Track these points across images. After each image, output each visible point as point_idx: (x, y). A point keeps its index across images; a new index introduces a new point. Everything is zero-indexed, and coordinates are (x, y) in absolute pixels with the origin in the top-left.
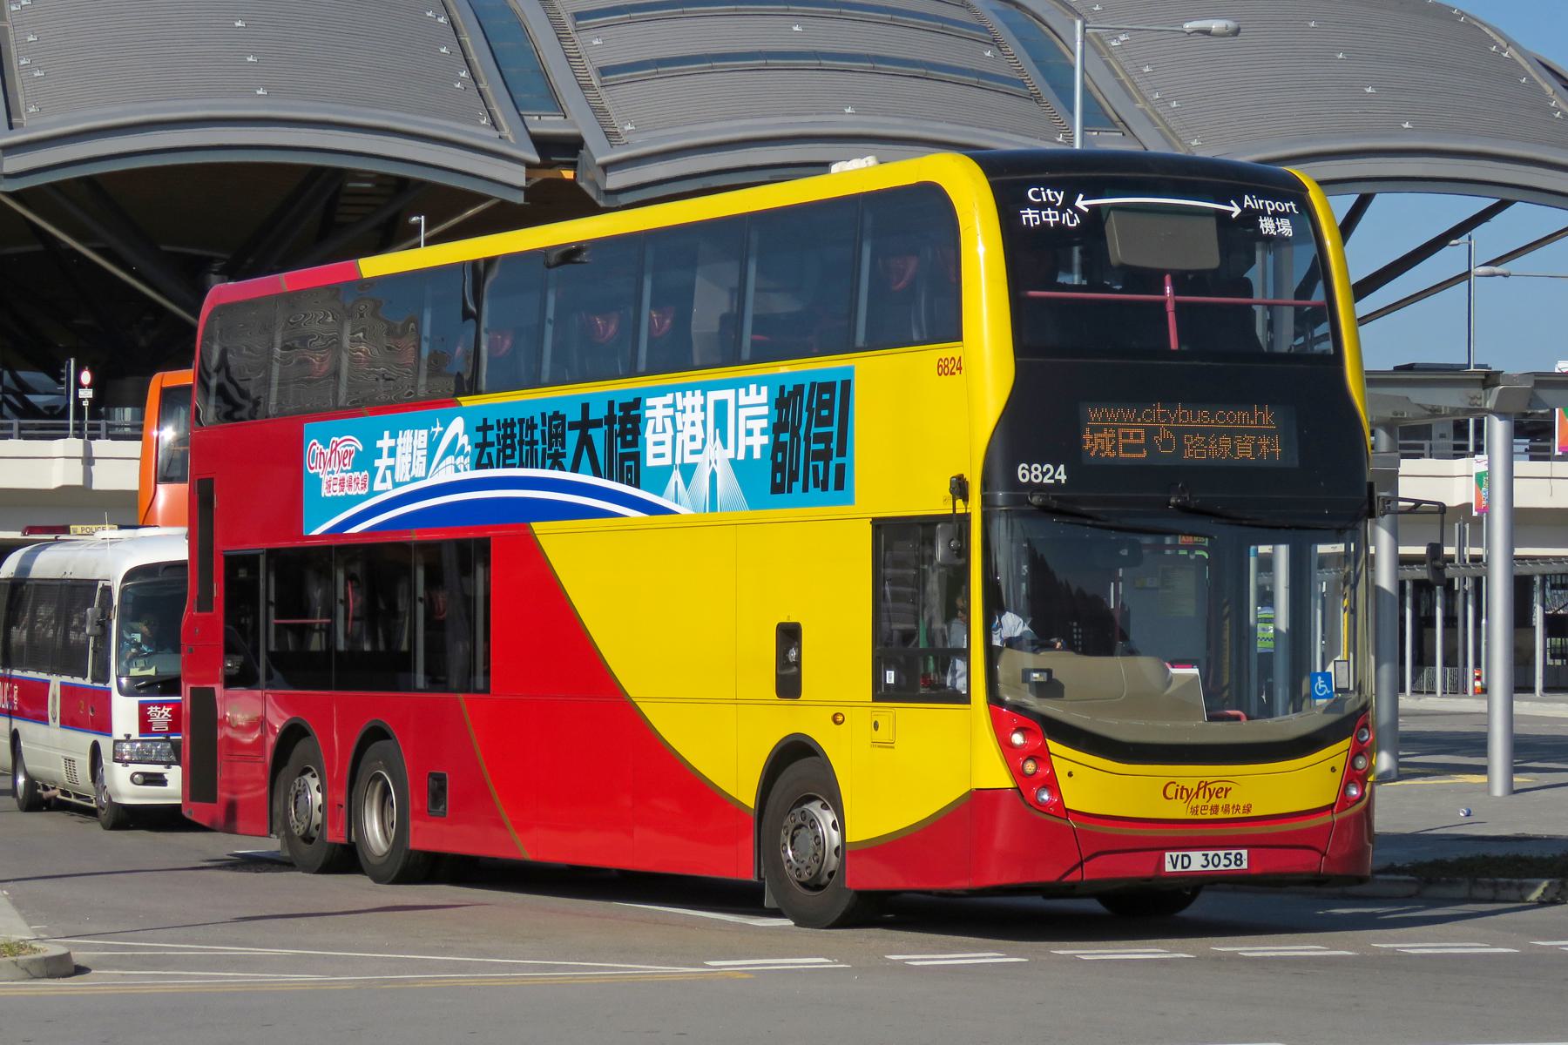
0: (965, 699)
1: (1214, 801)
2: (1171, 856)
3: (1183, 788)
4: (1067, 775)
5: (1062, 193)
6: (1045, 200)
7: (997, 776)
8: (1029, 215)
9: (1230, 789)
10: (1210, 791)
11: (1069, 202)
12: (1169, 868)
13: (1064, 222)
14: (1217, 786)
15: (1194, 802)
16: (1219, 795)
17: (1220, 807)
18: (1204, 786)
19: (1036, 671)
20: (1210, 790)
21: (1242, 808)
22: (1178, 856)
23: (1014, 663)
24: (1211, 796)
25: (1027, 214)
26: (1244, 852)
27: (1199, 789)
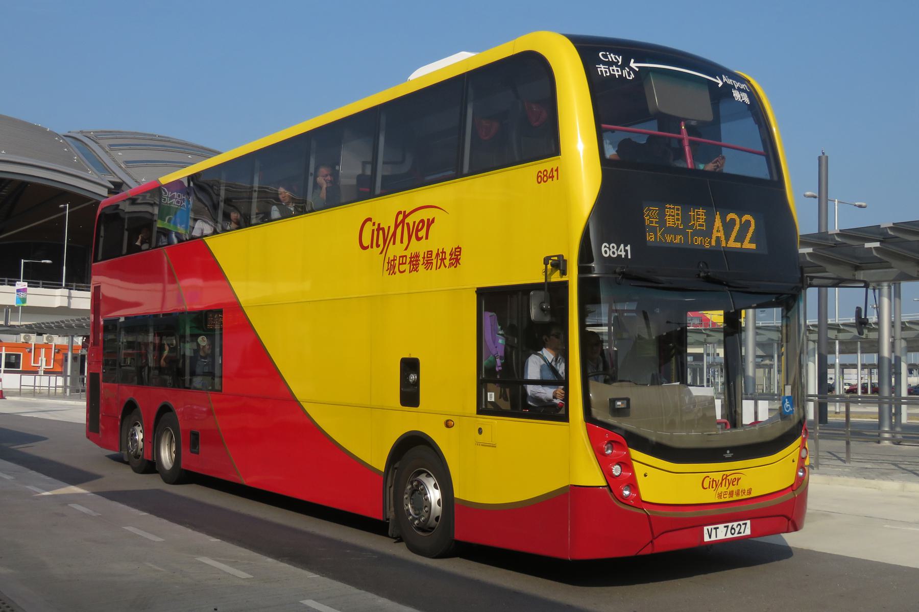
0: (565, 418)
1: (732, 488)
2: (708, 530)
3: (713, 481)
4: (643, 475)
5: (621, 57)
6: (611, 60)
7: (591, 476)
8: (602, 68)
9: (740, 479)
10: (728, 480)
11: (626, 64)
12: (706, 539)
13: (624, 76)
14: (733, 477)
15: (722, 489)
16: (734, 483)
17: (735, 491)
18: (725, 478)
19: (619, 399)
20: (728, 480)
21: (746, 491)
22: (712, 529)
23: (601, 392)
24: (729, 484)
25: (601, 68)
26: (748, 522)
27: (723, 480)
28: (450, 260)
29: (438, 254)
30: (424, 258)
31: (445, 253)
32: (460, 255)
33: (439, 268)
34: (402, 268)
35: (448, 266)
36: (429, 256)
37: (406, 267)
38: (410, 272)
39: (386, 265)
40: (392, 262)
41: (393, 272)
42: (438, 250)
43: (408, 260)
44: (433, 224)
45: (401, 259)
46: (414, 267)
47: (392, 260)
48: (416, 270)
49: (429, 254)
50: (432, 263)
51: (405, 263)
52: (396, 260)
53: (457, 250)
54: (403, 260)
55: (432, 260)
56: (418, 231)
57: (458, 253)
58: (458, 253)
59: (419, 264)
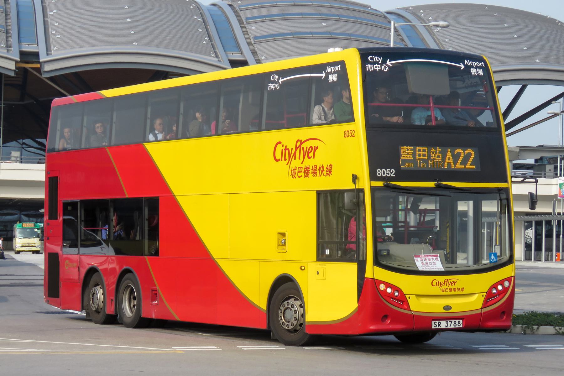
28: (326, 172)
29: (320, 168)
30: (312, 169)
31: (324, 167)
32: (331, 169)
33: (321, 176)
34: (300, 174)
35: (325, 174)
36: (315, 168)
37: (302, 174)
38: (304, 177)
39: (290, 172)
40: (294, 170)
41: (295, 176)
42: (320, 165)
43: (303, 170)
44: (317, 150)
45: (299, 169)
46: (307, 175)
47: (294, 169)
48: (308, 176)
49: (315, 167)
50: (317, 173)
51: (301, 172)
52: (296, 169)
53: (331, 166)
54: (300, 169)
55: (317, 171)
56: (309, 153)
57: (331, 168)
58: (330, 168)
59: (309, 173)
